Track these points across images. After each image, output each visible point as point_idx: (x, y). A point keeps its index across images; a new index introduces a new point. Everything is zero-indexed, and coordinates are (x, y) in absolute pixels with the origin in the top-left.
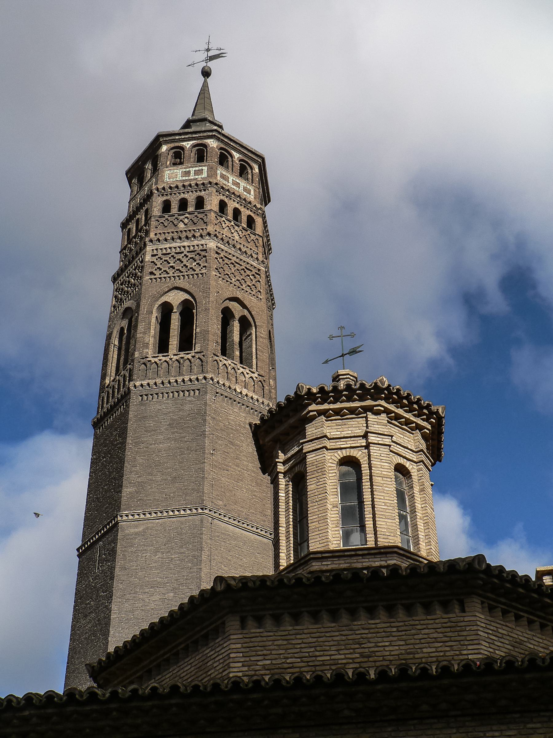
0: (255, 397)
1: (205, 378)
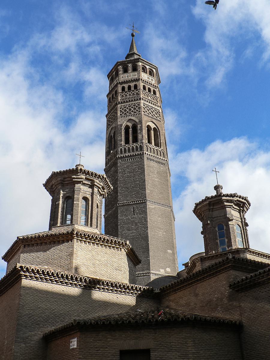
1: (143, 153)
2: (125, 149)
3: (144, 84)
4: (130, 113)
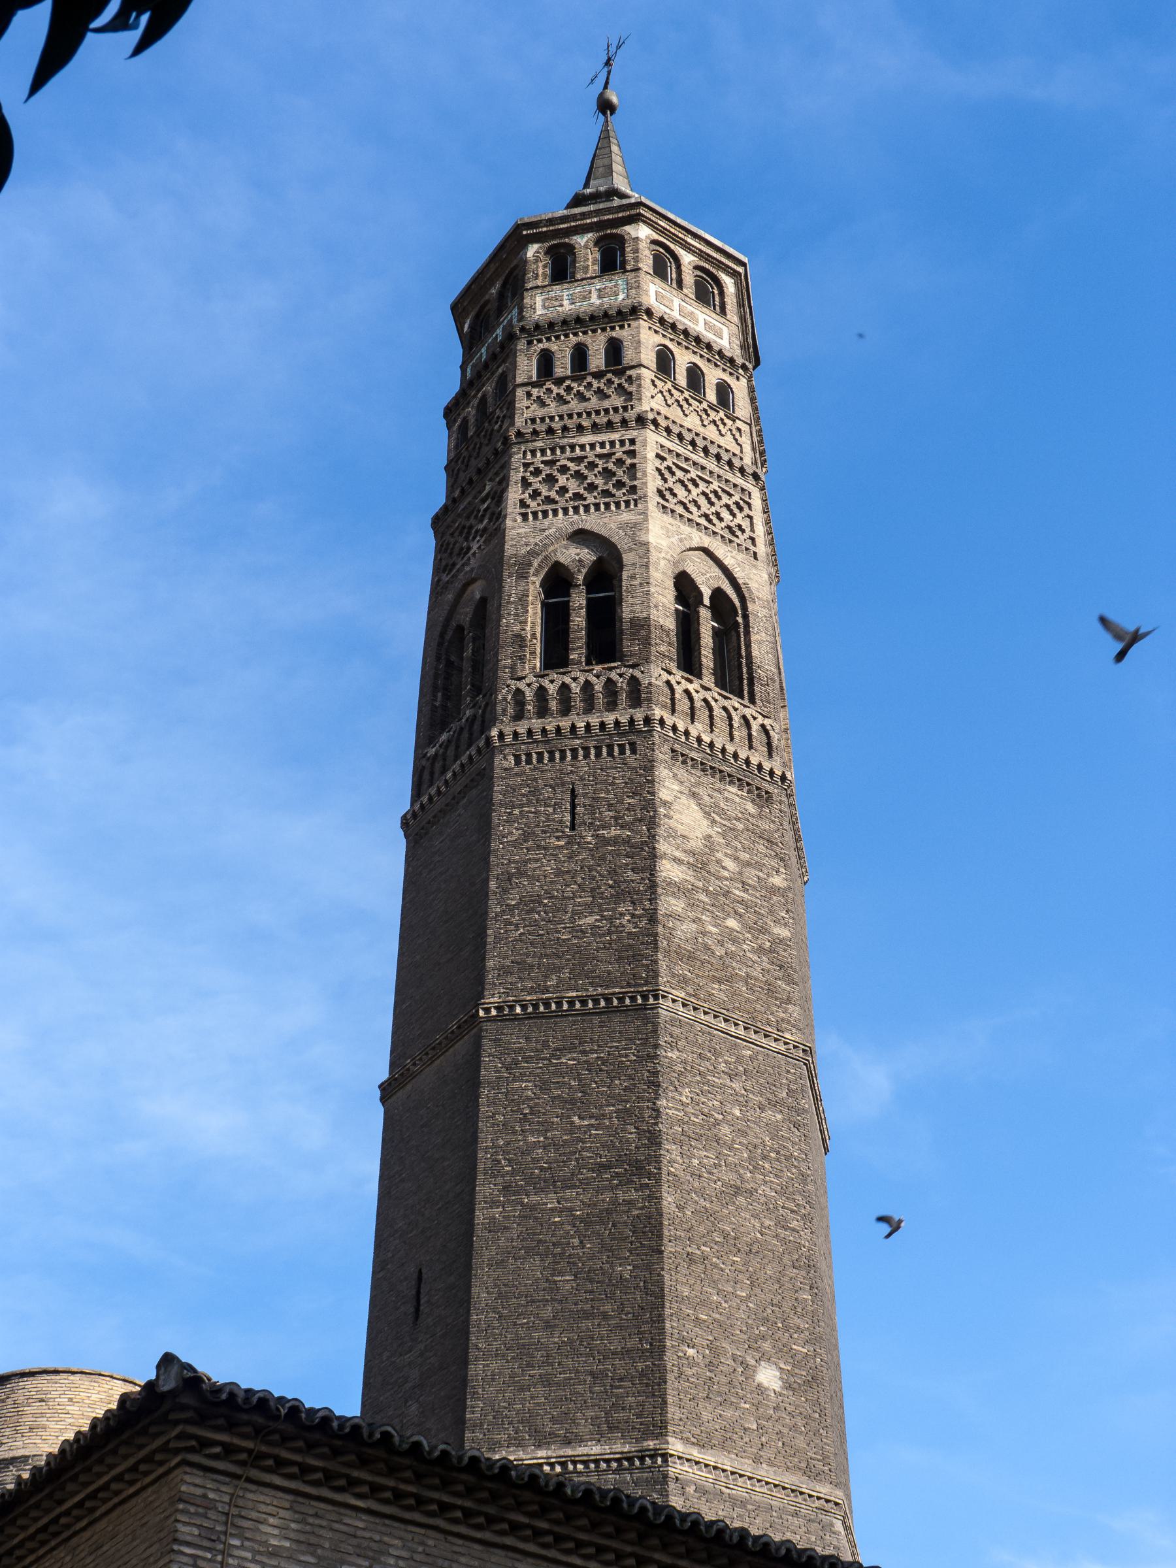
1: (648, 721)
2: (541, 692)
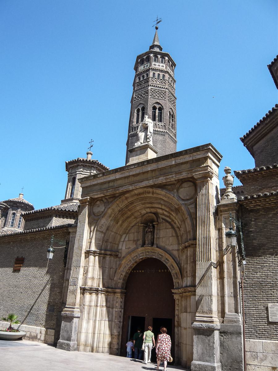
0: (162, 131)
3: (153, 72)
4: (138, 99)
